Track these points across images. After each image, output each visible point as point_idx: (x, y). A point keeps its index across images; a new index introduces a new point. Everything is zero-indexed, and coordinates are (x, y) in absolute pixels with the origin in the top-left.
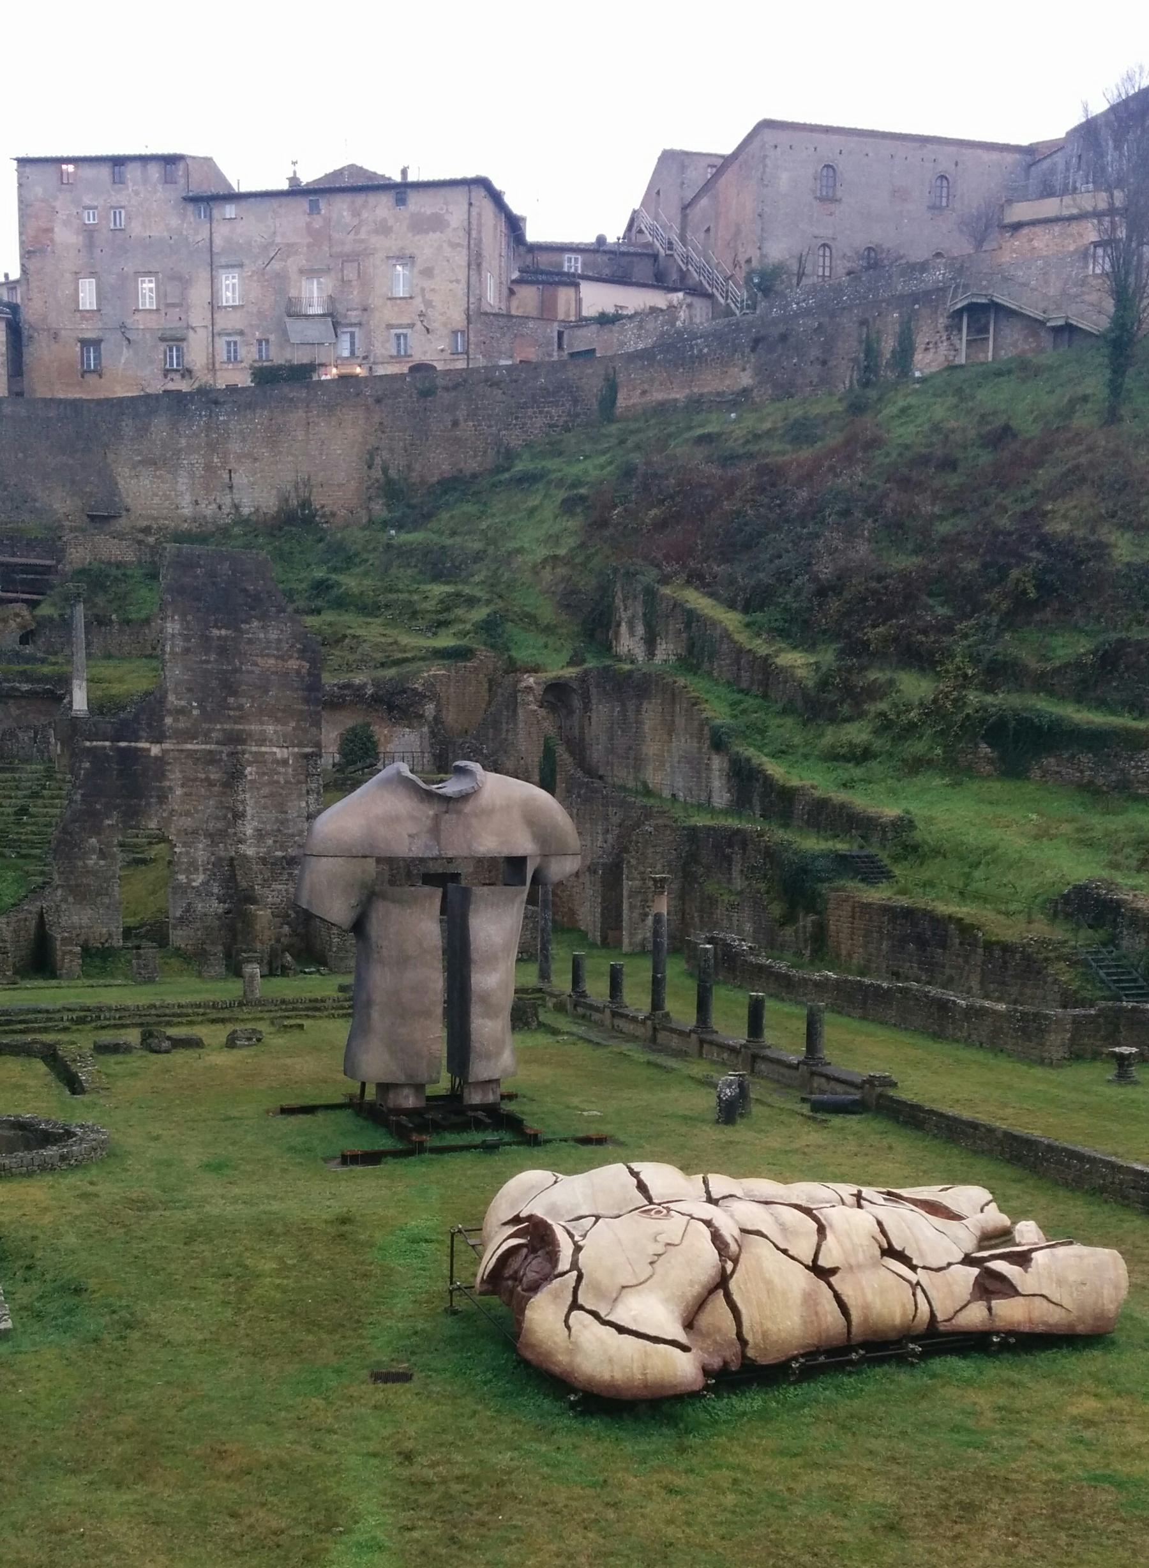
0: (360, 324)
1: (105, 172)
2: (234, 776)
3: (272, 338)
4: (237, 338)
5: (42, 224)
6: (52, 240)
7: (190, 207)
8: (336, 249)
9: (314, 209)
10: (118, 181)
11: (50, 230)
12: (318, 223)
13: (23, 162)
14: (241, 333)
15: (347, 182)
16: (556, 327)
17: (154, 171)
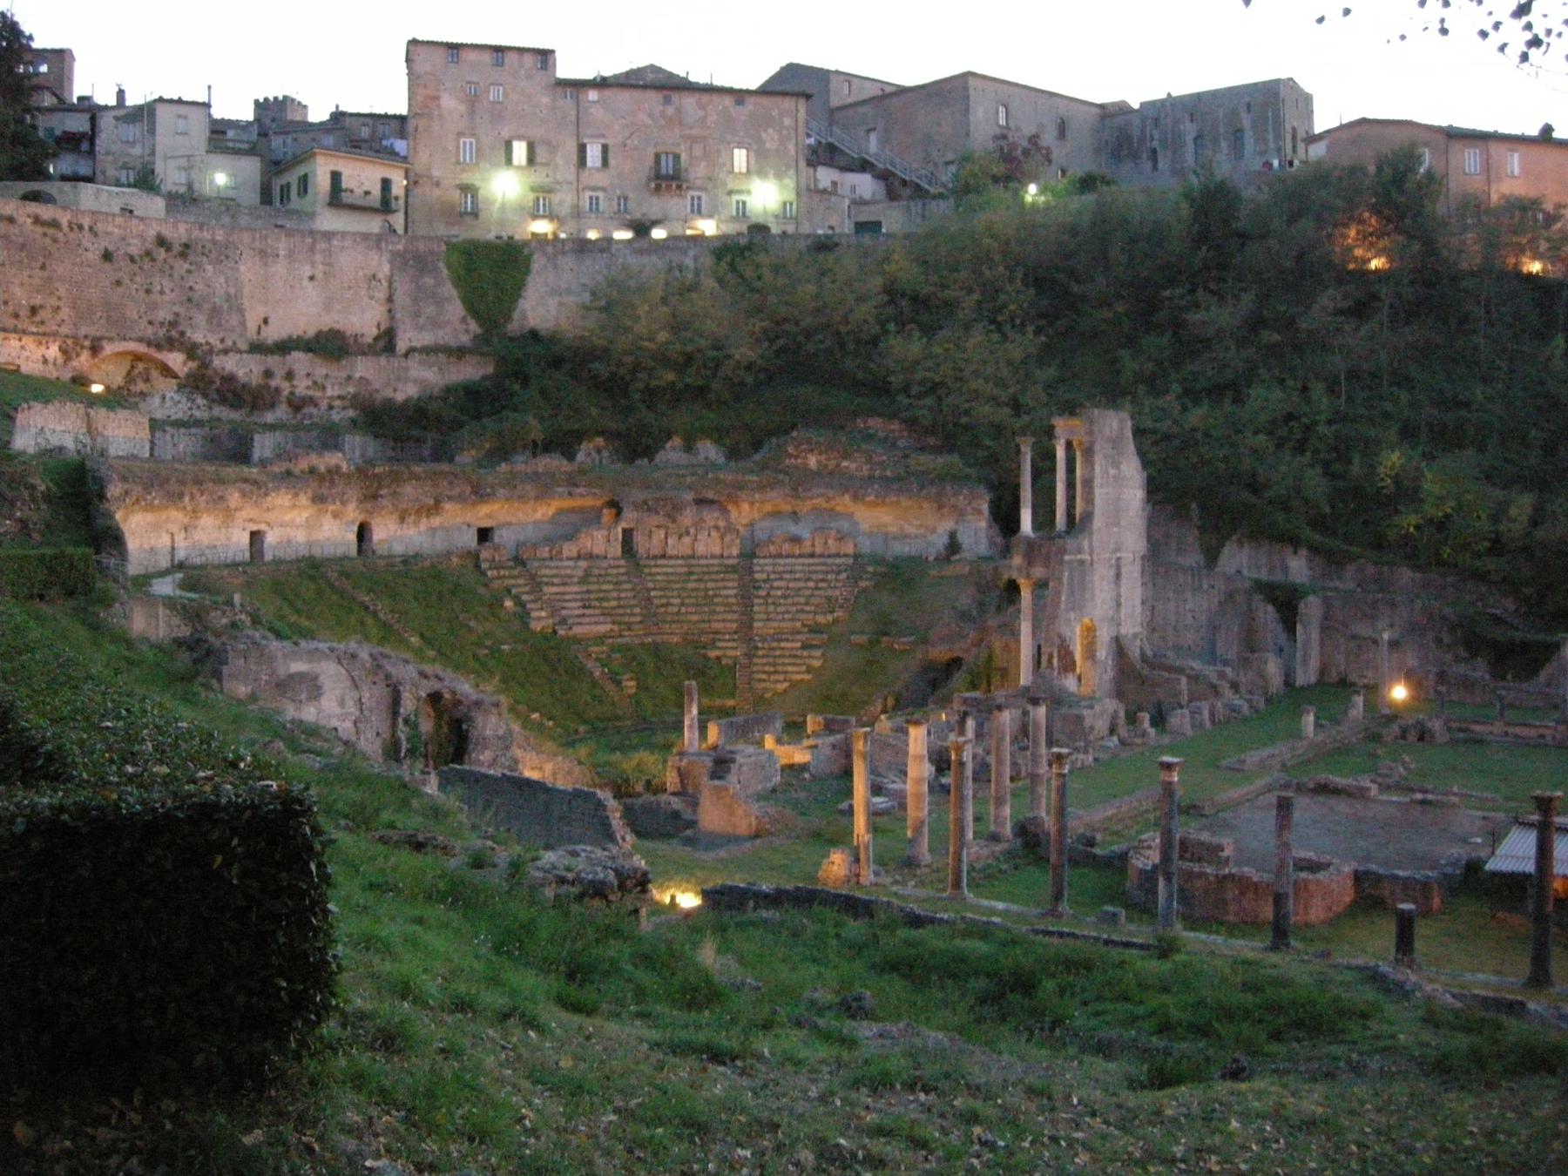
0: (704, 189)
1: (441, 51)
2: (1118, 576)
3: (631, 196)
4: (600, 194)
5: (430, 92)
6: (439, 106)
7: (559, 90)
8: (687, 132)
9: (667, 101)
10: (499, 63)
11: (437, 98)
12: (670, 110)
13: (413, 43)
14: (603, 189)
15: (650, 77)
16: (847, 202)
17: (528, 60)
